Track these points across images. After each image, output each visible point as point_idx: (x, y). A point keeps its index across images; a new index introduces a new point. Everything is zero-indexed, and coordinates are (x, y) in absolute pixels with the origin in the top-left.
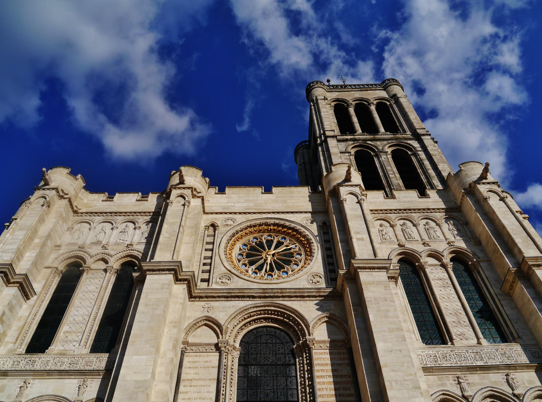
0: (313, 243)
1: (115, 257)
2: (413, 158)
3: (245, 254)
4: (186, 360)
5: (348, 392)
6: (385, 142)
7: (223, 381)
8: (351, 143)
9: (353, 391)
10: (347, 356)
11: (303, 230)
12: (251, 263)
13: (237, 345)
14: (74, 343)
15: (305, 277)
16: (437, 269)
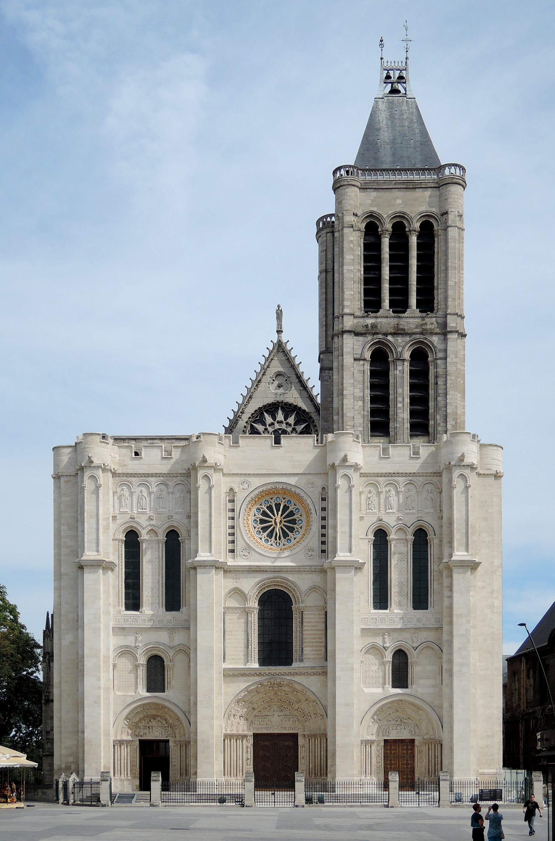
0: (311, 513)
1: (162, 528)
2: (431, 368)
3: (258, 520)
4: (227, 617)
5: (321, 640)
6: (408, 339)
7: (250, 632)
8: (370, 338)
9: (324, 640)
10: (324, 616)
11: (305, 497)
12: (264, 529)
13: (256, 605)
14: (155, 605)
15: (303, 550)
16: (401, 543)
